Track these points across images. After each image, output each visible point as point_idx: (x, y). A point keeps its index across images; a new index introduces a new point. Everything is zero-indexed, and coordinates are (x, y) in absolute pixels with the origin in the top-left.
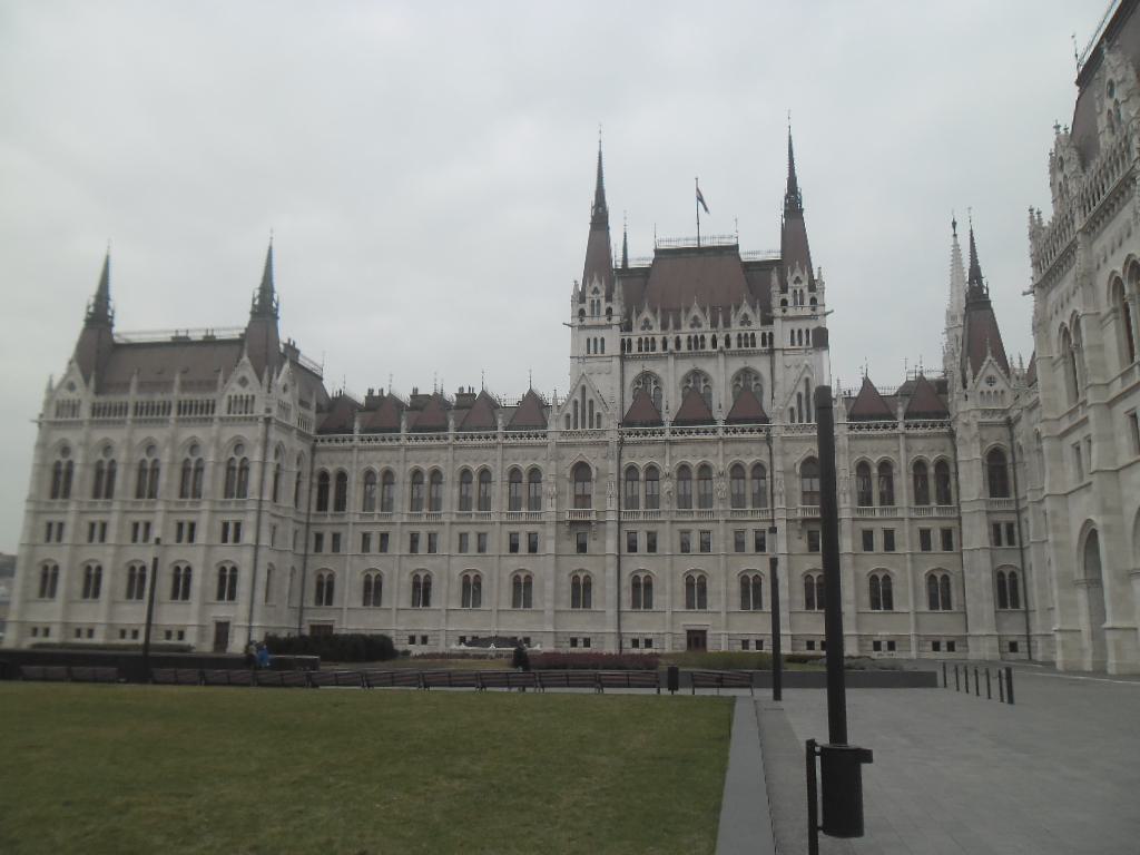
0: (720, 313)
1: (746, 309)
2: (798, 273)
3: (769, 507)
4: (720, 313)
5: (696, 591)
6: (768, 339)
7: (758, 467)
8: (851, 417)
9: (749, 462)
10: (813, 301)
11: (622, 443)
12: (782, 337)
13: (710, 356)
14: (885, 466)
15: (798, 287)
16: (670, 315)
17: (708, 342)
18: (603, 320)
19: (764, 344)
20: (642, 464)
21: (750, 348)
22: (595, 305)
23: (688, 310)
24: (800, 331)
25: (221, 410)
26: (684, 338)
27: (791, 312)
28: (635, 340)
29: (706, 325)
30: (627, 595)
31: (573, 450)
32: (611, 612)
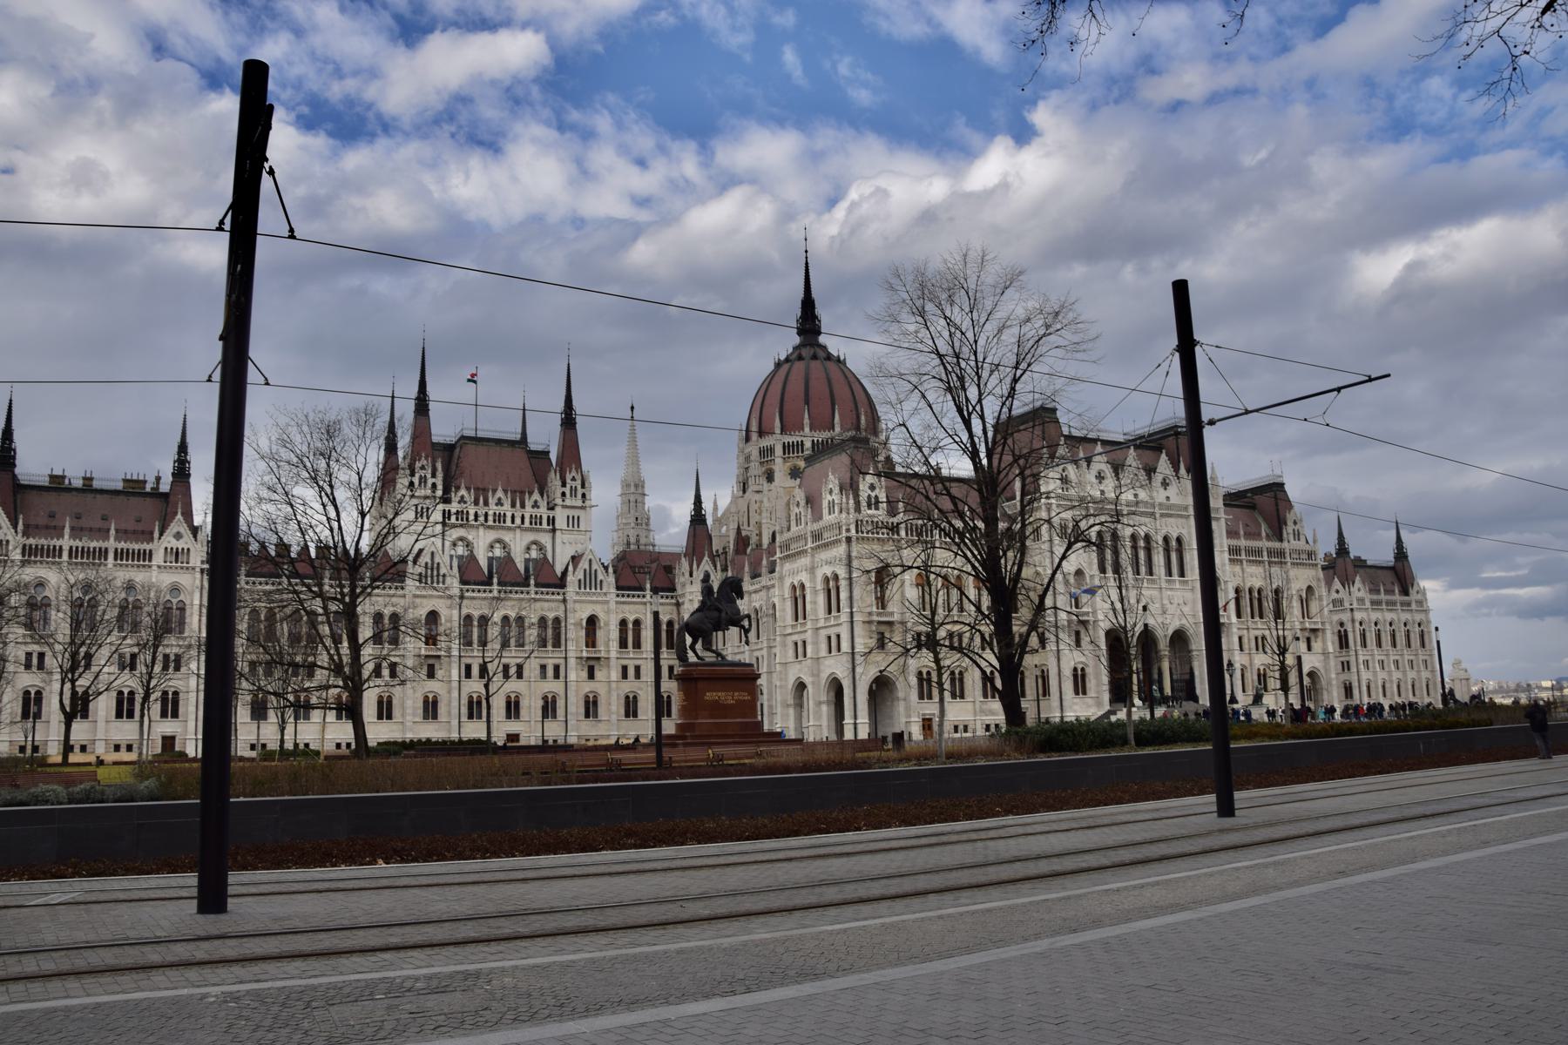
0: (518, 496)
1: (536, 496)
2: (574, 473)
4: (518, 496)
5: (513, 709)
6: (551, 521)
7: (557, 620)
8: (618, 588)
9: (551, 615)
10: (584, 495)
11: (462, 597)
12: (561, 523)
13: (509, 529)
14: (637, 623)
15: (574, 484)
16: (481, 494)
17: (509, 519)
20: (476, 614)
22: (423, 480)
23: (494, 491)
25: (158, 558)
27: (568, 502)
29: (507, 506)
30: (464, 710)
31: (425, 601)
32: (455, 722)
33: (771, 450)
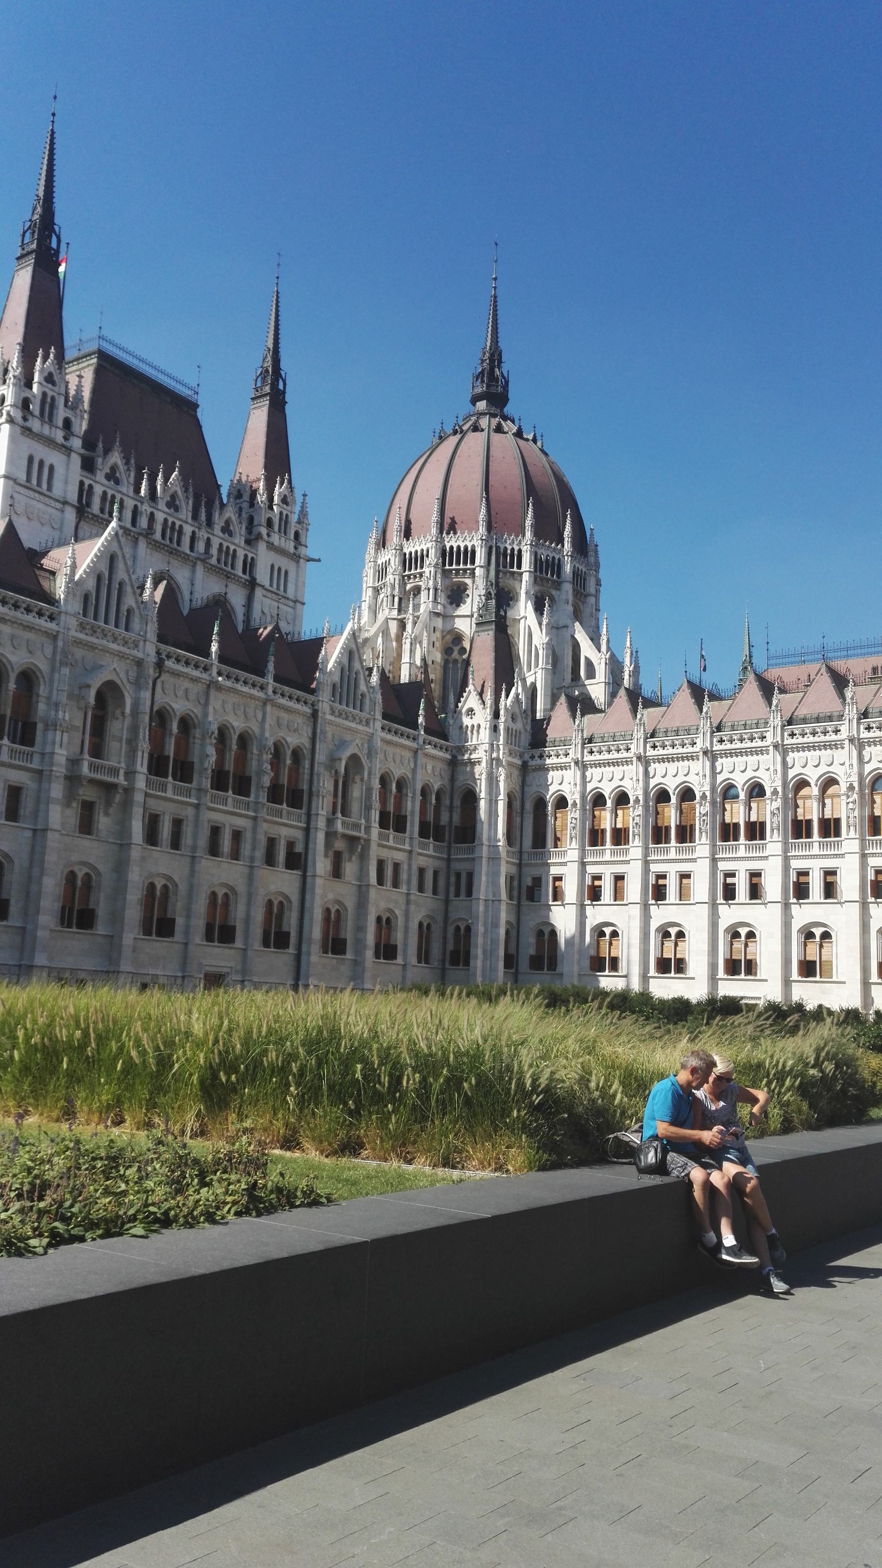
3: (304, 811)
6: (249, 566)
7: (297, 754)
8: (385, 716)
10: (297, 535)
11: (160, 665)
13: (185, 558)
17: (186, 540)
18: (59, 436)
19: (244, 572)
21: (229, 569)
24: (279, 569)
26: (160, 517)
27: (275, 539)
28: (98, 490)
29: (186, 513)
33: (469, 555)
